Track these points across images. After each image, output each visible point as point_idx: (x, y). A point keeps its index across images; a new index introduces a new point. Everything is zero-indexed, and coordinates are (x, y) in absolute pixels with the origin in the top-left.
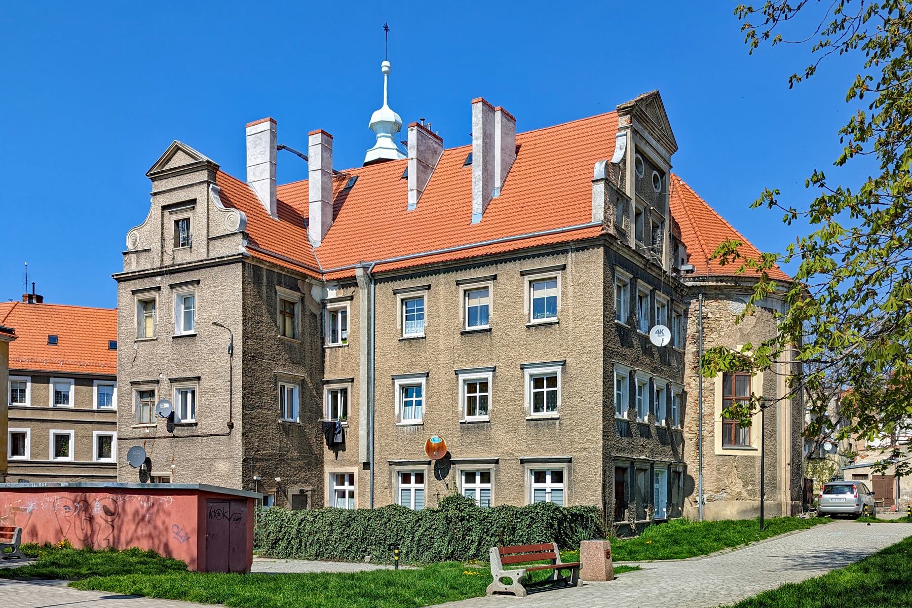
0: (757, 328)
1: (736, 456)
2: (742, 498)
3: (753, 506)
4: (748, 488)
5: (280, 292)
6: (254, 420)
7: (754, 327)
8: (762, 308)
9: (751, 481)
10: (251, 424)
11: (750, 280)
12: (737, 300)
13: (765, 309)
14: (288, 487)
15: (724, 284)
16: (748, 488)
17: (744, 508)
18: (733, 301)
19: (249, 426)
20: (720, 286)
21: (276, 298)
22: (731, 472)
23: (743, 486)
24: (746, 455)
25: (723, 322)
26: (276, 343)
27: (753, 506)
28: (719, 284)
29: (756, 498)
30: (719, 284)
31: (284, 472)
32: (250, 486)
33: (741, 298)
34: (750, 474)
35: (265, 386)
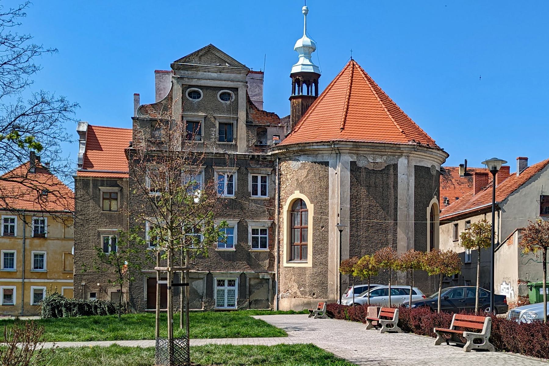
0: (309, 177)
1: (293, 268)
2: (297, 296)
3: (304, 302)
4: (301, 290)
5: (102, 189)
6: (82, 255)
7: (306, 177)
8: (312, 162)
9: (303, 285)
10: (80, 258)
11: (293, 146)
12: (295, 160)
13: (315, 163)
14: (108, 288)
15: (281, 151)
16: (301, 290)
17: (297, 303)
18: (293, 161)
19: (78, 259)
20: (282, 152)
21: (100, 193)
22: (291, 278)
23: (298, 288)
24: (299, 266)
25: (288, 177)
26: (99, 215)
27: (304, 302)
28: (280, 151)
29: (306, 296)
30: (280, 151)
31: (105, 281)
32: (79, 288)
33: (297, 158)
34: (302, 280)
35: (91, 237)
